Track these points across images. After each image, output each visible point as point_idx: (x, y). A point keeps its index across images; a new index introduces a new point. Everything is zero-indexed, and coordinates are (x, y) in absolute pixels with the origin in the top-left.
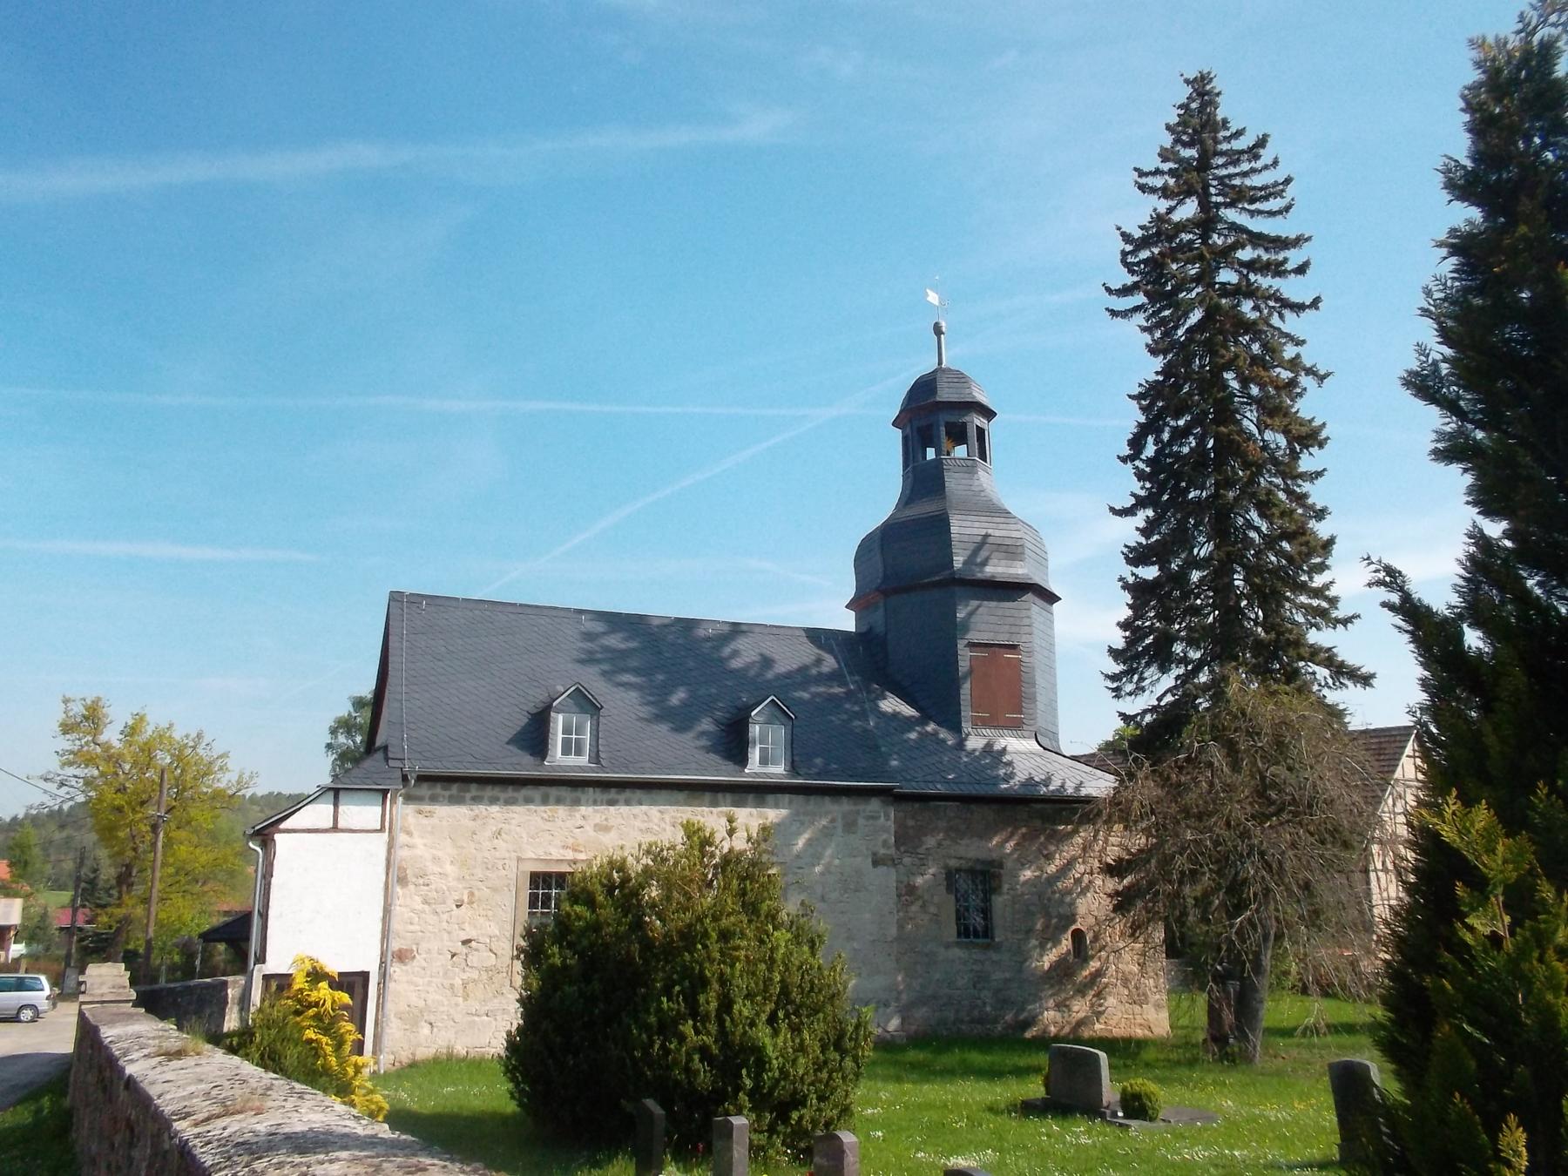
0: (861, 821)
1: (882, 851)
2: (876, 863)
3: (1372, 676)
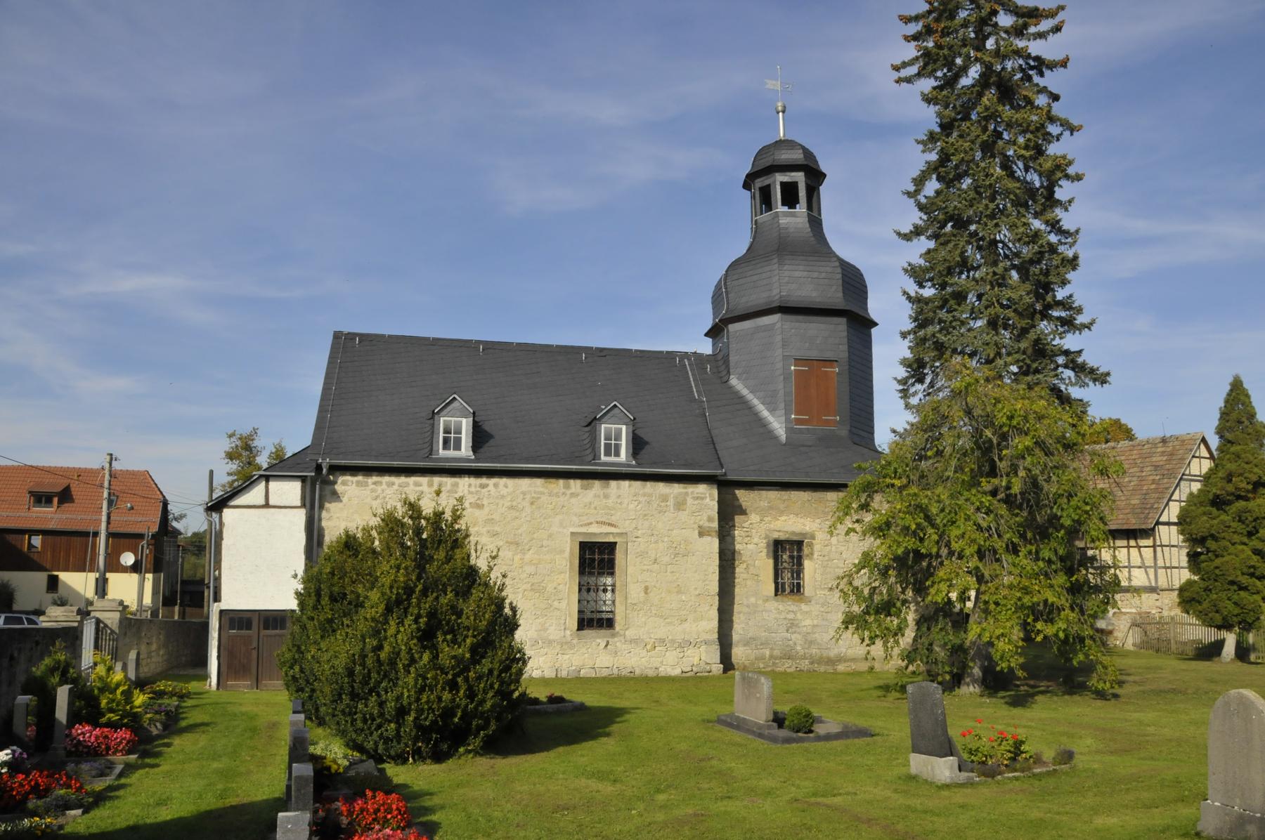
0: (689, 501)
1: (707, 524)
2: (701, 534)
3: (1108, 374)
